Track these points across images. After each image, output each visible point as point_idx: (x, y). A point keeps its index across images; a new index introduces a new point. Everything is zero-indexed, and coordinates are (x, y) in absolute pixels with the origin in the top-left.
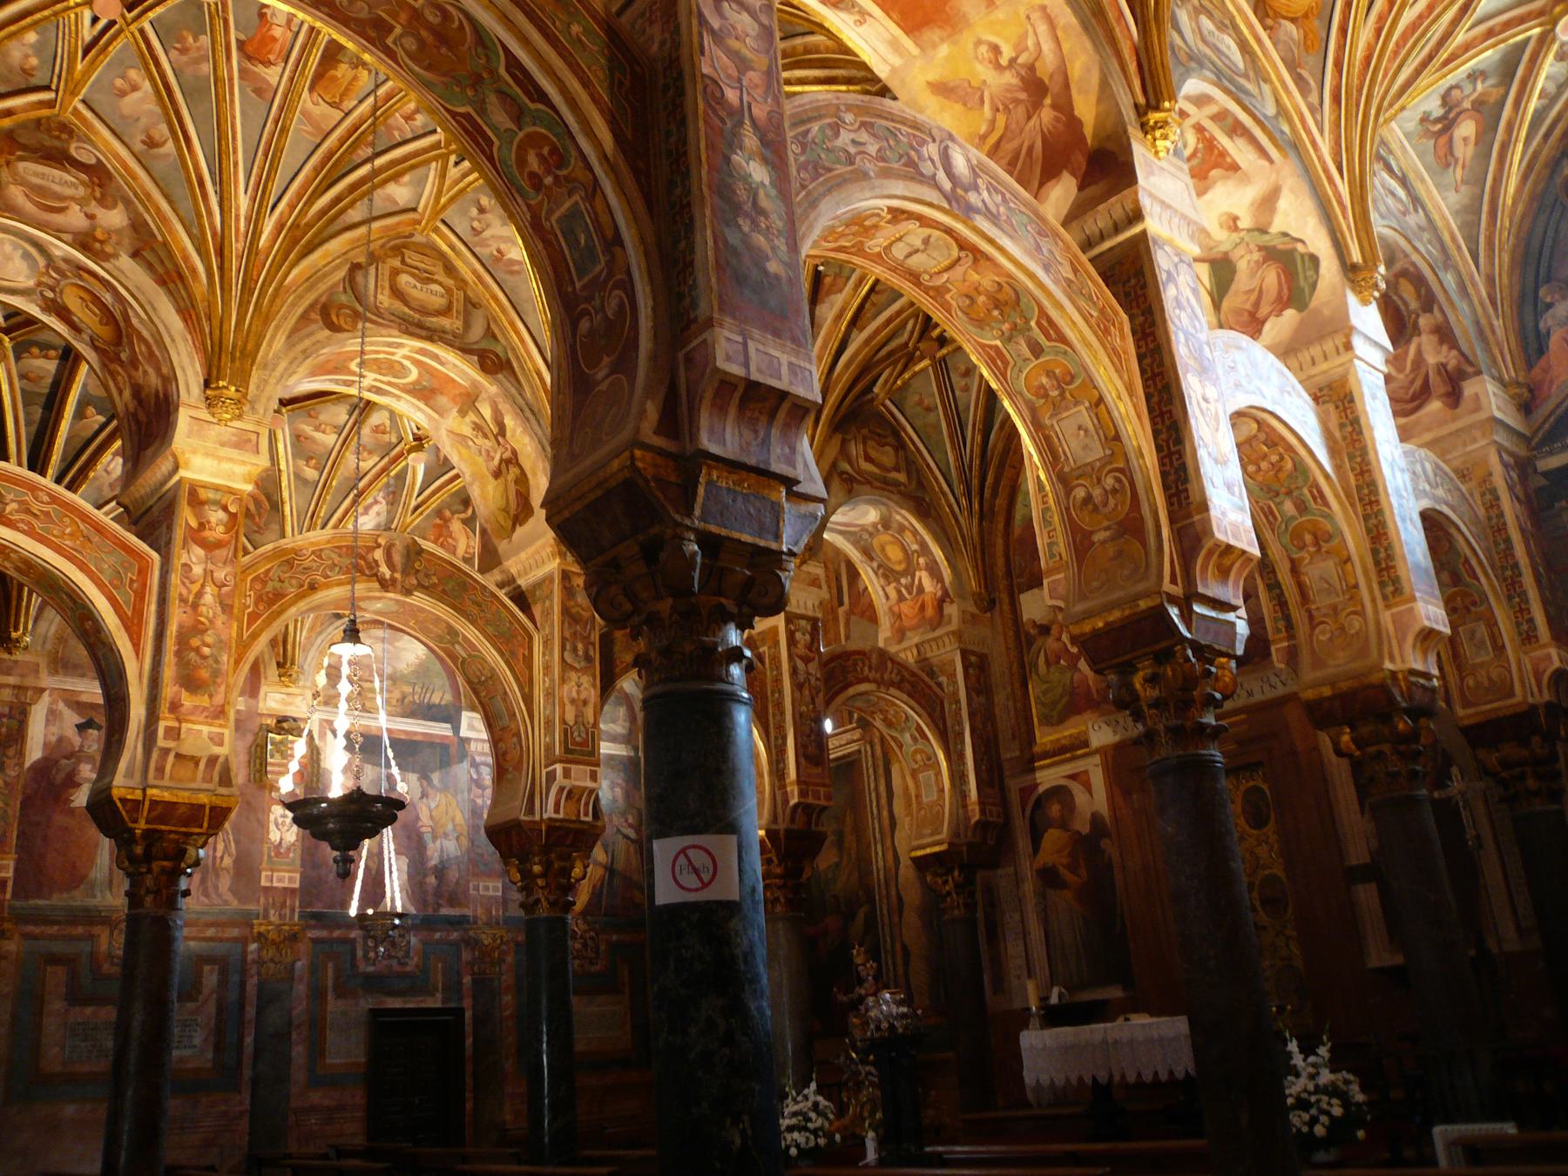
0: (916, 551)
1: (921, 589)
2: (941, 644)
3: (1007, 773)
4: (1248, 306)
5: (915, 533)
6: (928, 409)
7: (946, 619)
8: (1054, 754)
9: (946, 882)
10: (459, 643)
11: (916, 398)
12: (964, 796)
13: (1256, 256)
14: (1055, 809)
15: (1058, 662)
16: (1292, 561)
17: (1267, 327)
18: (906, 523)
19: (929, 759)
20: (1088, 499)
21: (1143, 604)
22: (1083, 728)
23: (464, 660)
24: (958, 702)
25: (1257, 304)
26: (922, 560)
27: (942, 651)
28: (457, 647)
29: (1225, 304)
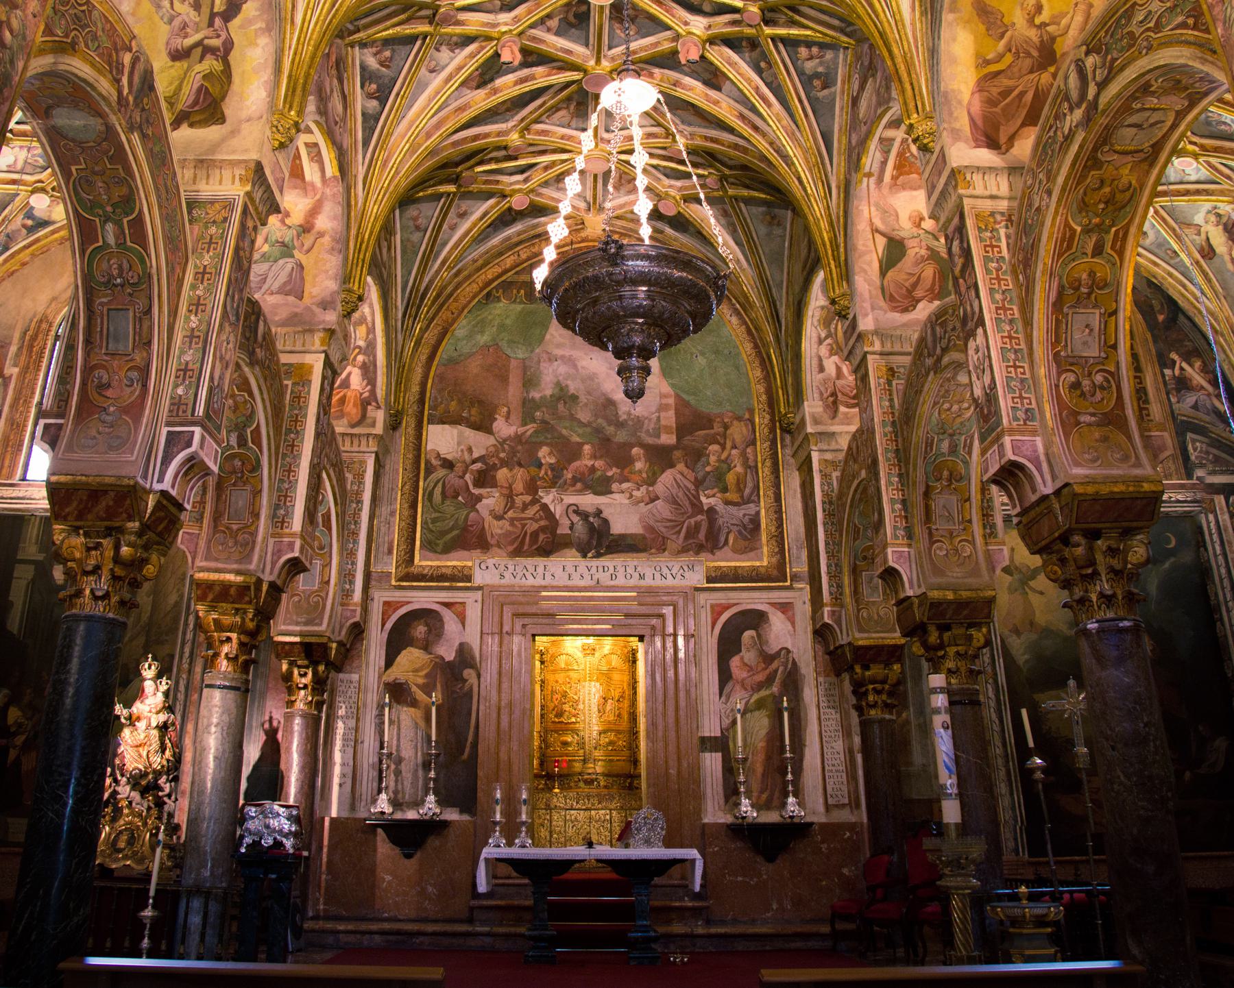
0: (359, 347)
1: (346, 384)
2: (356, 442)
3: (373, 583)
4: (907, 284)
5: (371, 330)
6: (418, 228)
7: (369, 421)
8: (432, 579)
9: (305, 675)
10: (118, 224)
11: (415, 213)
12: (348, 594)
13: (923, 252)
14: (420, 630)
15: (456, 497)
16: (928, 487)
17: (920, 305)
18: (369, 319)
19: (321, 548)
20: (1076, 386)
21: (1147, 487)
22: (470, 564)
23: (106, 245)
24: (360, 502)
25: (915, 285)
26: (360, 358)
27: (357, 449)
28: (110, 227)
29: (890, 274)
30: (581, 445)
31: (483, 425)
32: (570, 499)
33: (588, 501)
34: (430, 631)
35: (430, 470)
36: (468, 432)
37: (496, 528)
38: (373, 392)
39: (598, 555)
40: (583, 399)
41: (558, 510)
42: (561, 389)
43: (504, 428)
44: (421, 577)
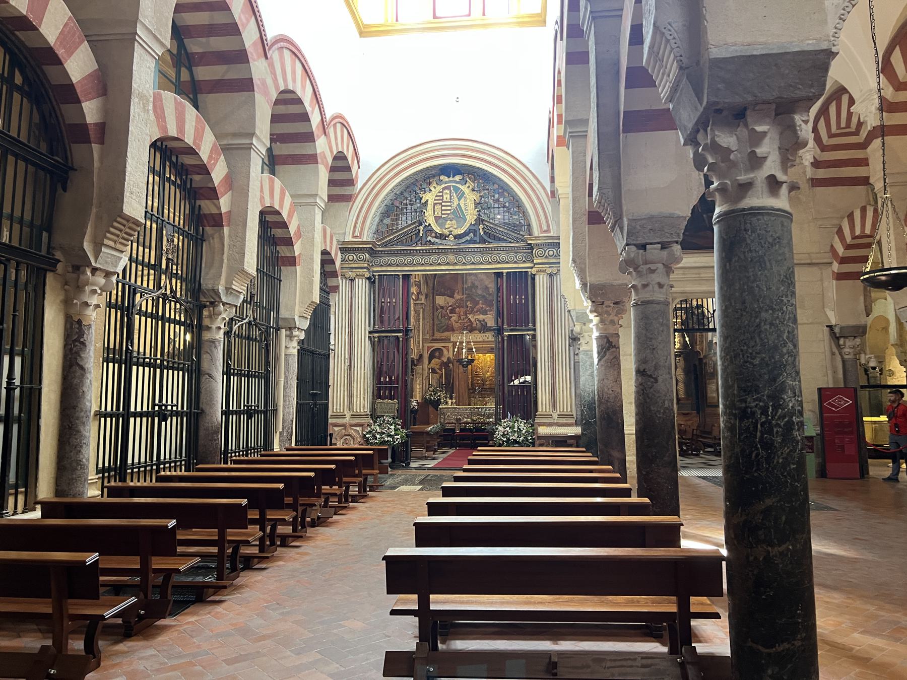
14: (437, 354)
30: (479, 301)
31: (452, 296)
32: (476, 317)
33: (481, 317)
34: (440, 354)
35: (437, 309)
36: (447, 298)
37: (456, 326)
38: (420, 290)
39: (484, 332)
40: (479, 287)
41: (473, 320)
42: (473, 284)
43: (457, 297)
44: (437, 340)
